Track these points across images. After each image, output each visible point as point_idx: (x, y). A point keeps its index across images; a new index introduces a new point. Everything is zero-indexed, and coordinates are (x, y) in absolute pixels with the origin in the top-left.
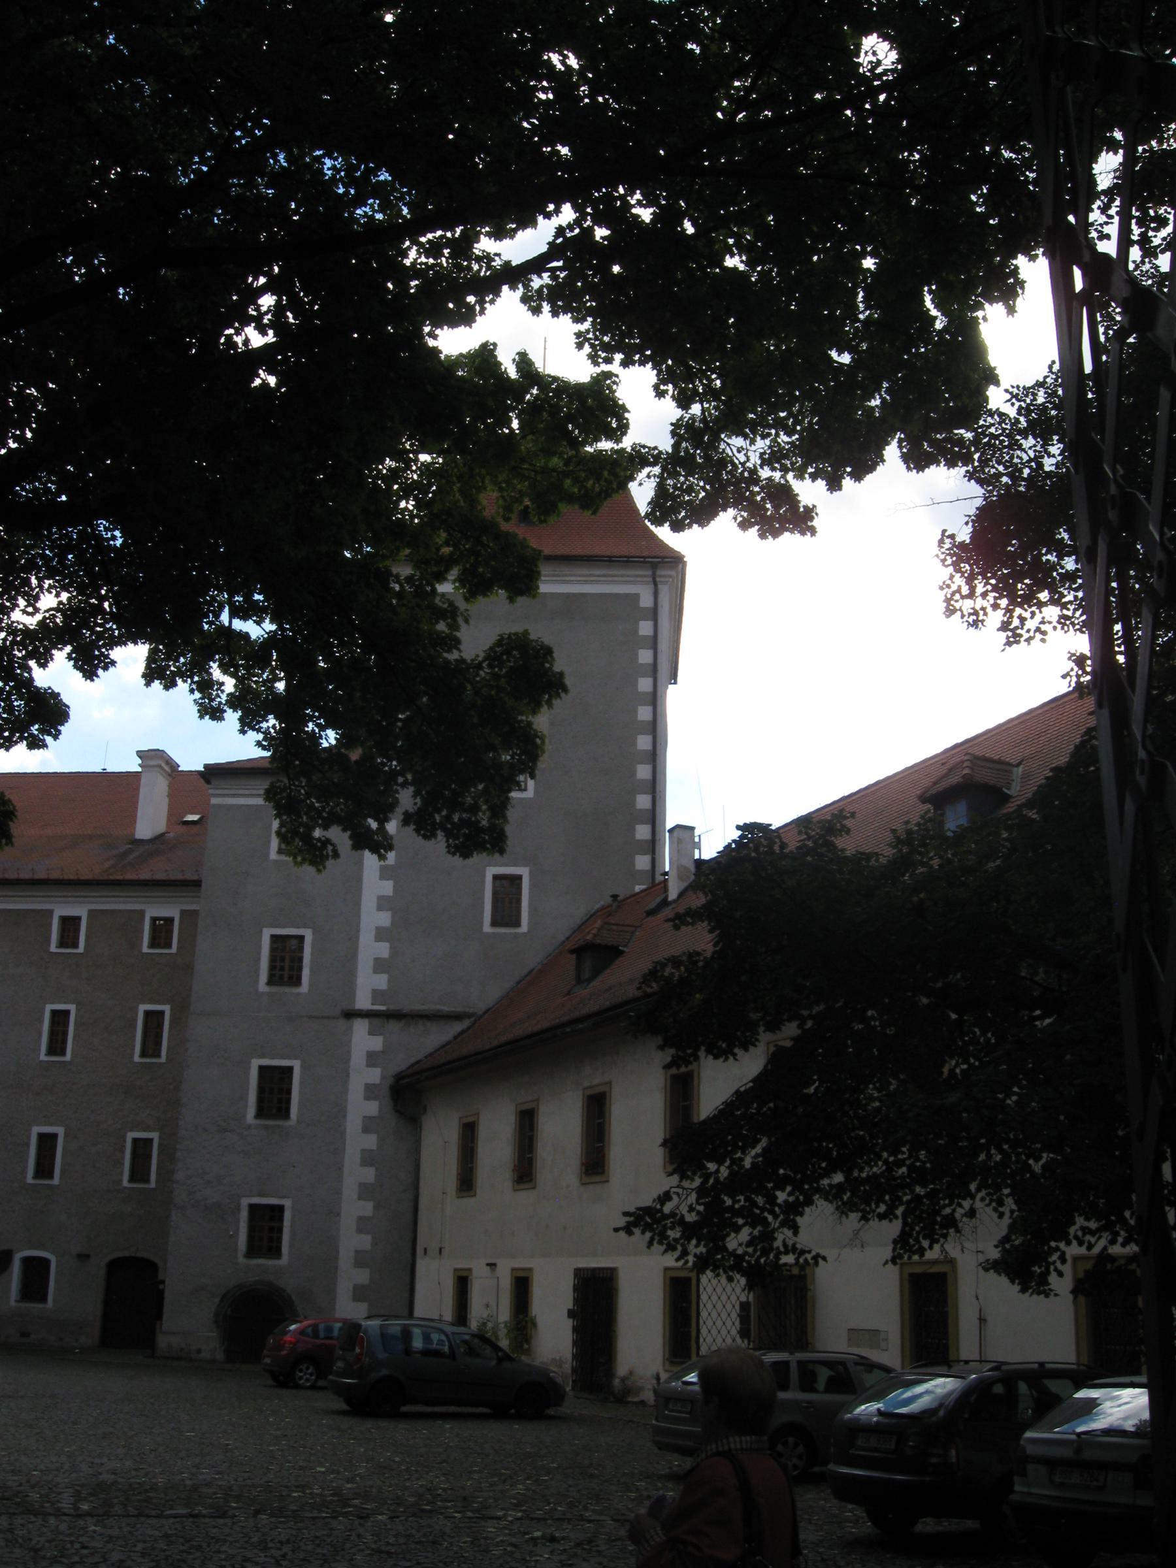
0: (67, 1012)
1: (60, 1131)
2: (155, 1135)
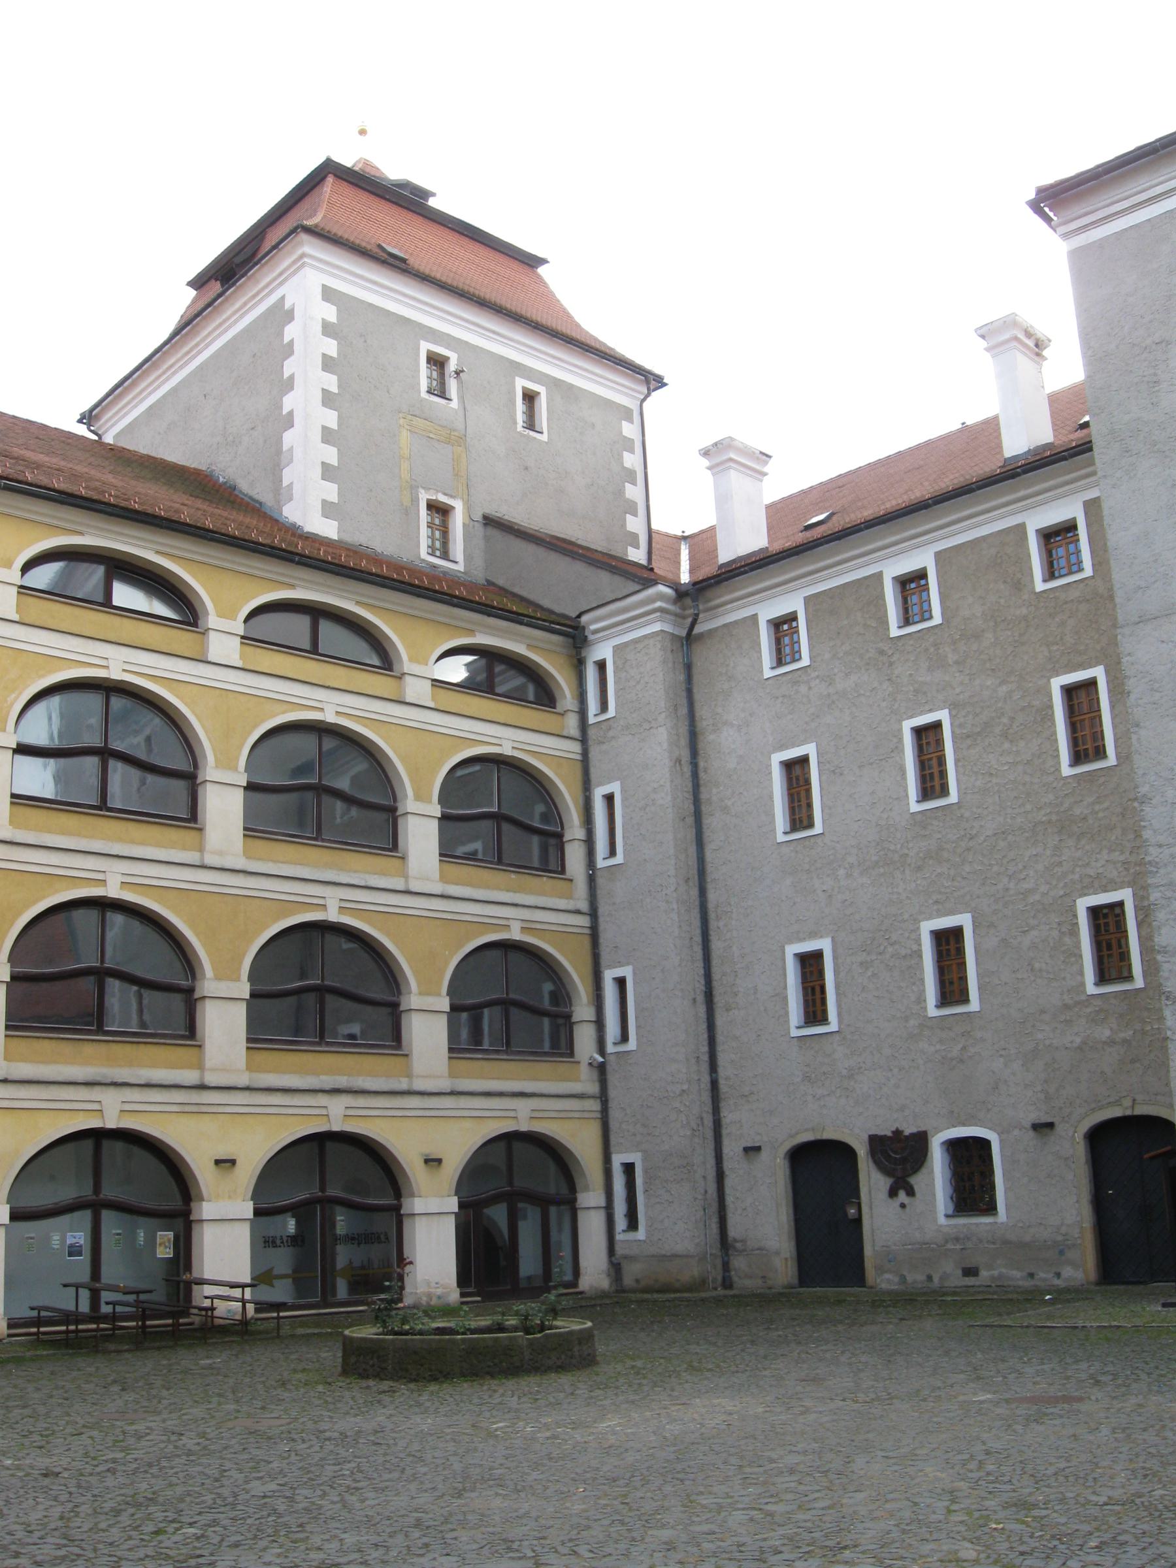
0: (937, 726)
1: (964, 920)
2: (1125, 895)
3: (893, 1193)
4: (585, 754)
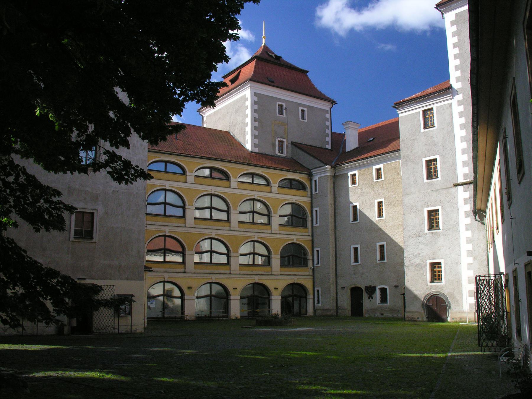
3: (369, 298)
4: (312, 200)
